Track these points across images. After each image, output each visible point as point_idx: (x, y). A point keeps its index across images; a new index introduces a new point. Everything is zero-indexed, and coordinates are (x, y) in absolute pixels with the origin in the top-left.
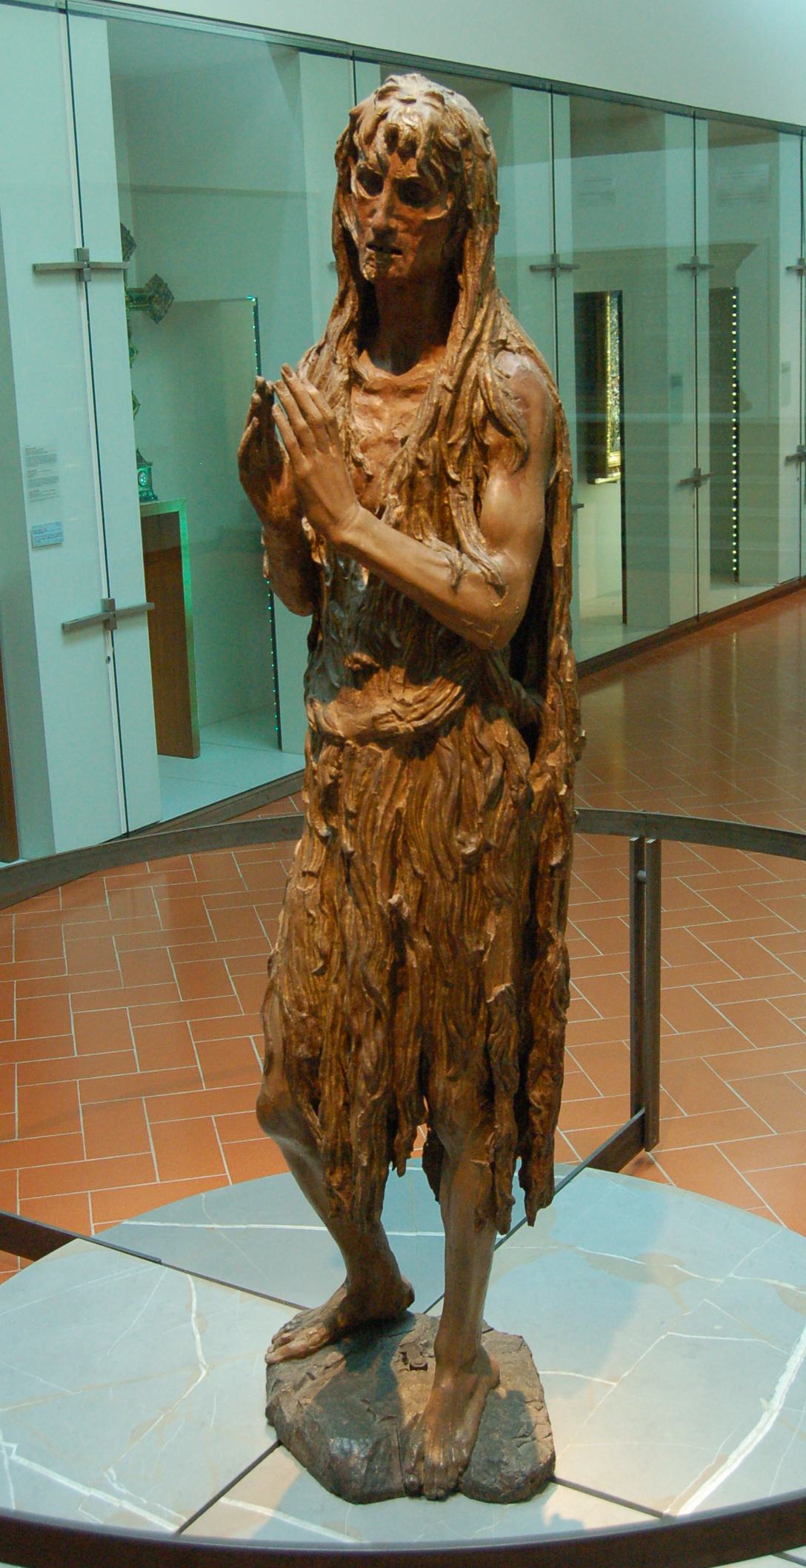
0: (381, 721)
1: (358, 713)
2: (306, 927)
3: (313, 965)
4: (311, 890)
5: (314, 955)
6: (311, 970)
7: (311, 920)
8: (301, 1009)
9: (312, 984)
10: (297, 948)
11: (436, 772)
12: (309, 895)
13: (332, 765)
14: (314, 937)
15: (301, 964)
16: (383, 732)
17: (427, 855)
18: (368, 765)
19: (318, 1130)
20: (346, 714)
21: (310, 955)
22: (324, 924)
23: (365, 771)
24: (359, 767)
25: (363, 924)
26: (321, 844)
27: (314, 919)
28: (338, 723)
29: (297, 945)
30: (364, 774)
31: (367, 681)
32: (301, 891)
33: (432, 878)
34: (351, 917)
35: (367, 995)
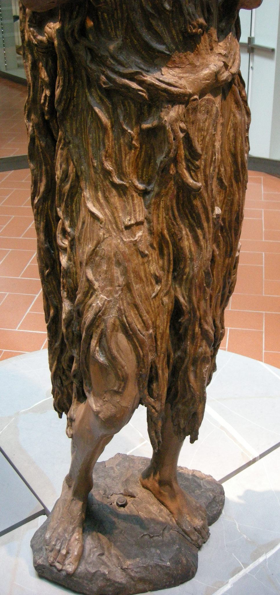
0: (221, 73)
1: (198, 72)
2: (142, 267)
3: (151, 292)
4: (142, 236)
5: (151, 284)
6: (151, 296)
7: (146, 260)
8: (147, 329)
9: (153, 305)
10: (137, 286)
11: (233, 106)
12: (140, 240)
13: (182, 121)
14: (150, 271)
15: (143, 295)
16: (223, 81)
17: (229, 170)
18: (208, 112)
19: (153, 404)
20: (187, 75)
21: (148, 286)
22: (154, 255)
23: (207, 118)
24: (201, 116)
25: (204, 238)
26: (139, 198)
27: (149, 258)
28: (183, 82)
29: (136, 284)
30: (206, 120)
31: (199, 44)
32: (131, 241)
33: (231, 185)
34: (188, 239)
35: (206, 288)
